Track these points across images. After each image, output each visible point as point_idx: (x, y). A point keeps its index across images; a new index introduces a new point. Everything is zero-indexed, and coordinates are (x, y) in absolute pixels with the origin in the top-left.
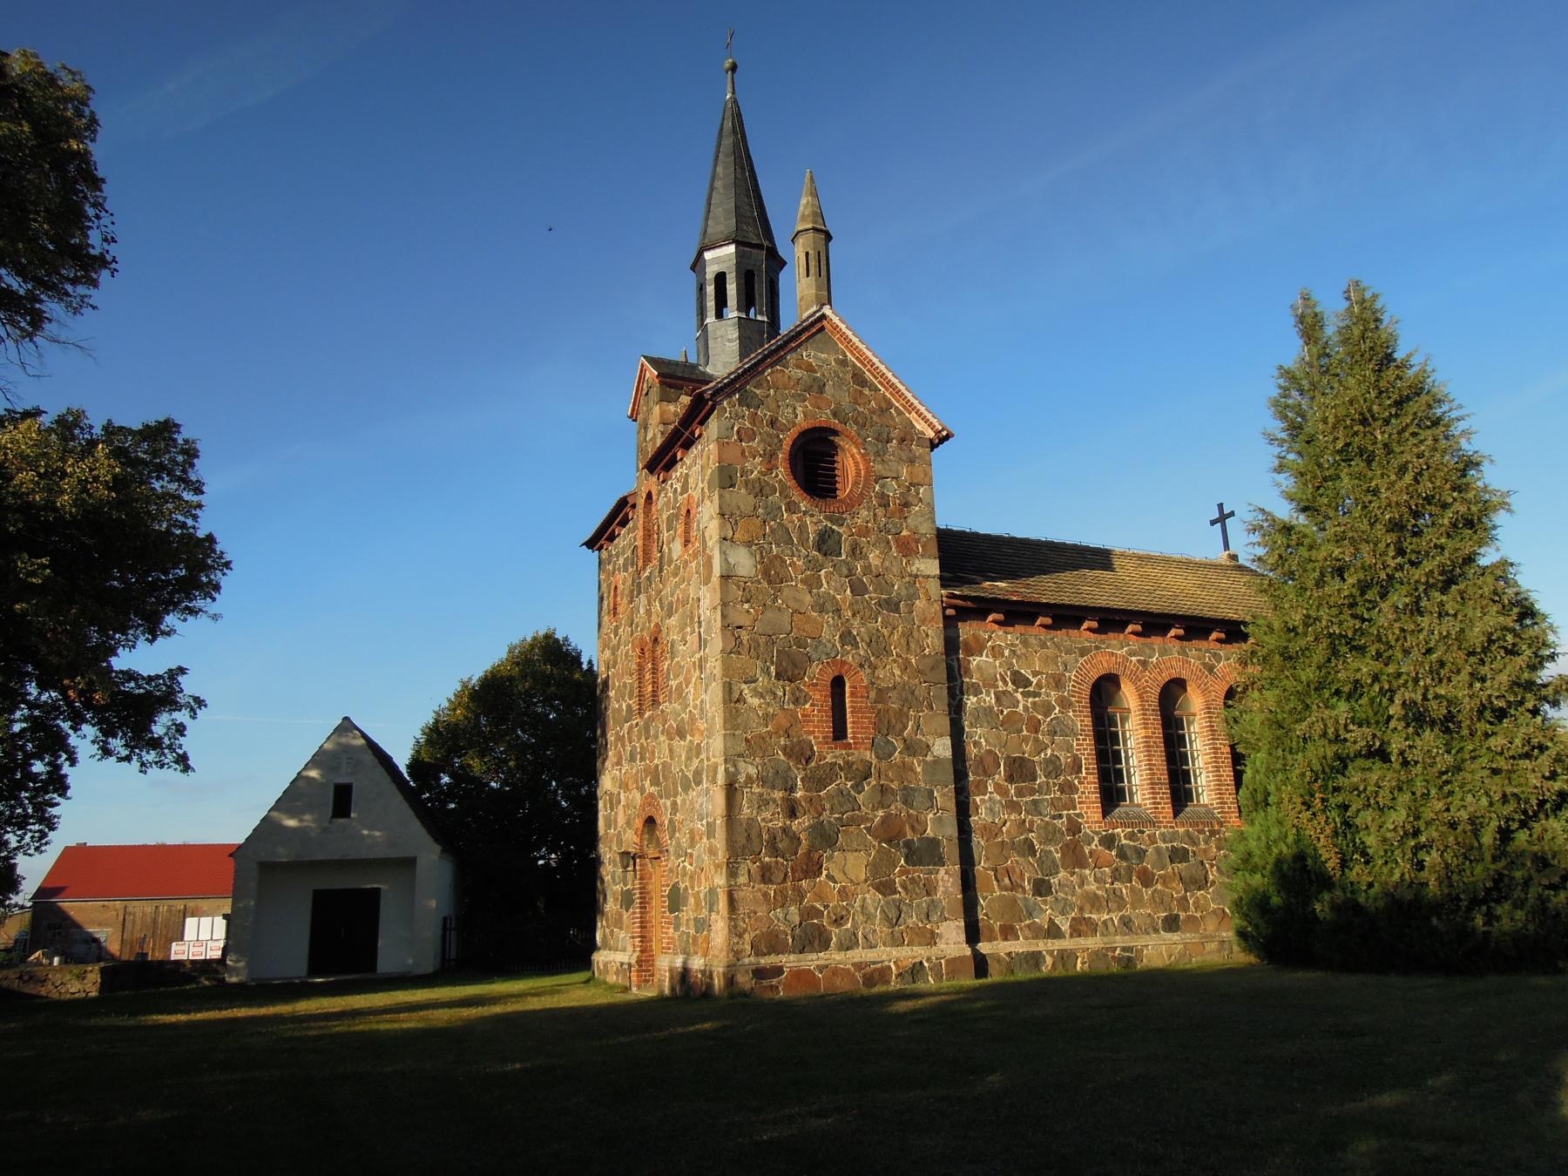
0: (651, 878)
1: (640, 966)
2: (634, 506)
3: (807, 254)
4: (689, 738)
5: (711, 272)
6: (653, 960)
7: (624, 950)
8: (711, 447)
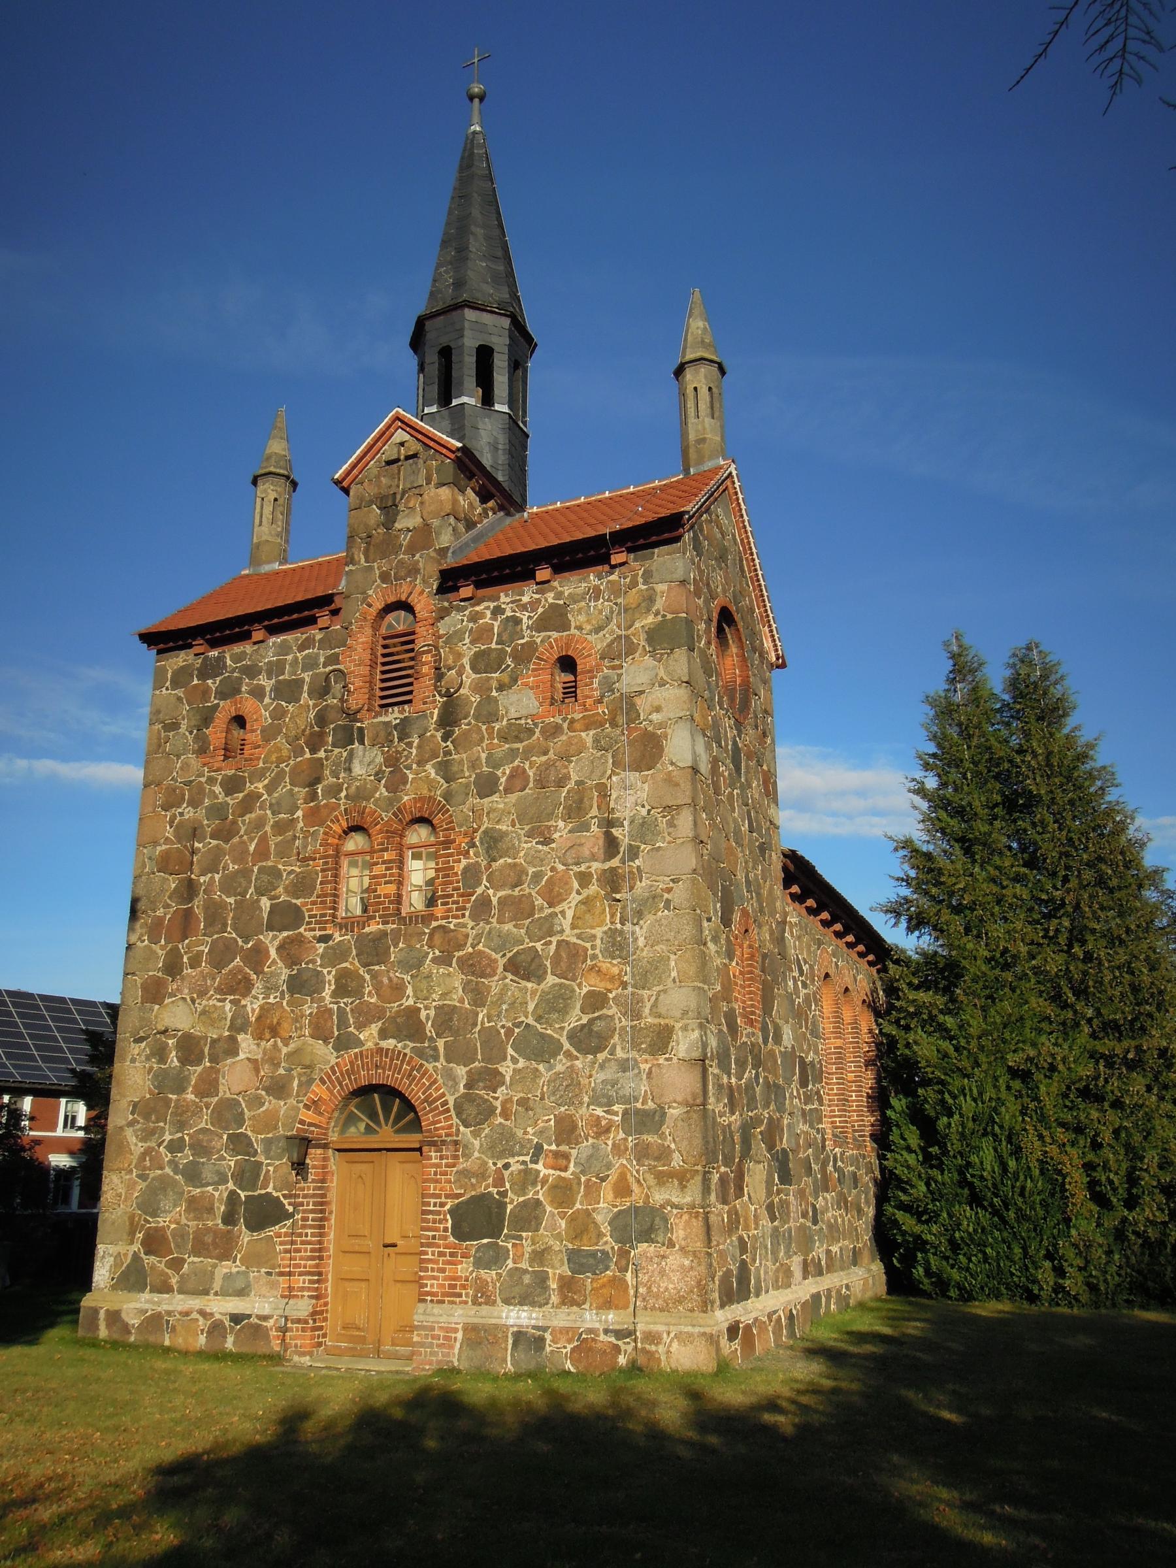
0: (332, 1182)
1: (315, 1321)
2: (335, 612)
3: (710, 389)
4: (551, 980)
5: (470, 342)
6: (327, 1311)
7: (242, 1293)
8: (661, 587)
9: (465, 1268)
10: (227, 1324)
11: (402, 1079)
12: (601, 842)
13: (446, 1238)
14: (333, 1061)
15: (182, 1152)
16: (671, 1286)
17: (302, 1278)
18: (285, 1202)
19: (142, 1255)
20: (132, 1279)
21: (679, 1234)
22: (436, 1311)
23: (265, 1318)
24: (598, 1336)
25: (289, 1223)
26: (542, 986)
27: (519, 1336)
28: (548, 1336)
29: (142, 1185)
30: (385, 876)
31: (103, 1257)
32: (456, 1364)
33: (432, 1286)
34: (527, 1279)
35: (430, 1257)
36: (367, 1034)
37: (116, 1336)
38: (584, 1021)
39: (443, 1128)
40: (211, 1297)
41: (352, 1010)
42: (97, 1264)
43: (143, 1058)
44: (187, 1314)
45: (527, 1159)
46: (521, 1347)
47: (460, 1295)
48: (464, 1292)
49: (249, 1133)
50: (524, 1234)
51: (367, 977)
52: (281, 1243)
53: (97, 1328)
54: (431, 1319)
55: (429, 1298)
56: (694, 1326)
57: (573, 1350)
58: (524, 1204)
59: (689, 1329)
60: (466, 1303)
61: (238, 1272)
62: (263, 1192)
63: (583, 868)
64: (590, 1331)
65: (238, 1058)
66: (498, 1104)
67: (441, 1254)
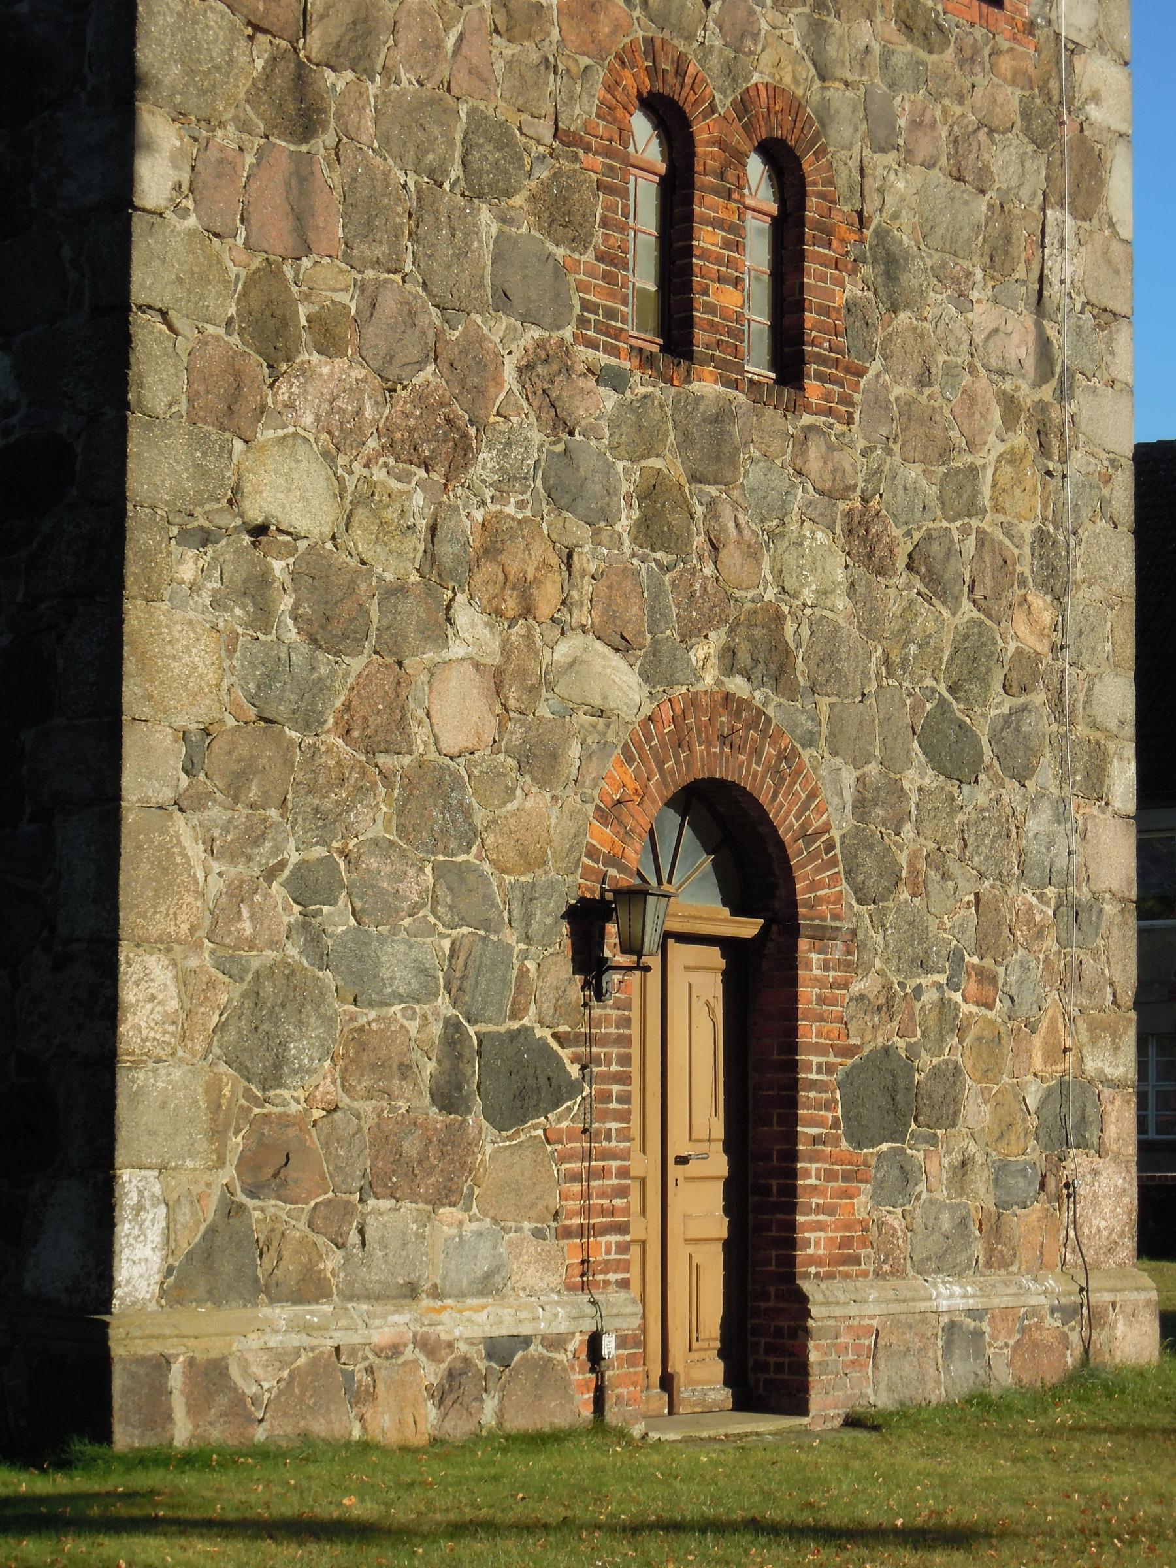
9: (862, 1204)
10: (482, 1365)
11: (764, 777)
12: (1031, 338)
13: (836, 1142)
14: (647, 710)
15: (332, 902)
16: (1103, 1224)
17: (603, 1240)
18: (565, 1054)
19: (241, 1197)
20: (227, 1268)
21: (1112, 1130)
22: (842, 1297)
23: (556, 1342)
24: (1042, 1320)
25: (573, 1104)
26: (956, 620)
27: (952, 1328)
28: (986, 1328)
29: (228, 993)
30: (719, 260)
31: (139, 1208)
32: (872, 1399)
33: (817, 1243)
34: (946, 1223)
35: (813, 1181)
36: (701, 654)
37: (216, 1434)
38: (1005, 710)
39: (826, 900)
40: (426, 1302)
41: (673, 584)
42: (125, 1229)
43: (205, 598)
44: (395, 1350)
45: (942, 978)
46: (957, 1353)
47: (856, 1260)
48: (863, 1252)
49: (487, 867)
50: (939, 1132)
51: (699, 510)
52: (563, 1159)
53: (169, 1417)
54: (838, 1311)
55: (813, 1270)
56: (1137, 1289)
57: (1014, 1349)
58: (936, 1072)
59: (1134, 1296)
60: (865, 1274)
61: (480, 1234)
62: (515, 1025)
63: (1008, 386)
64: (1034, 1311)
65: (446, 655)
66: (903, 859)
67: (831, 1175)
